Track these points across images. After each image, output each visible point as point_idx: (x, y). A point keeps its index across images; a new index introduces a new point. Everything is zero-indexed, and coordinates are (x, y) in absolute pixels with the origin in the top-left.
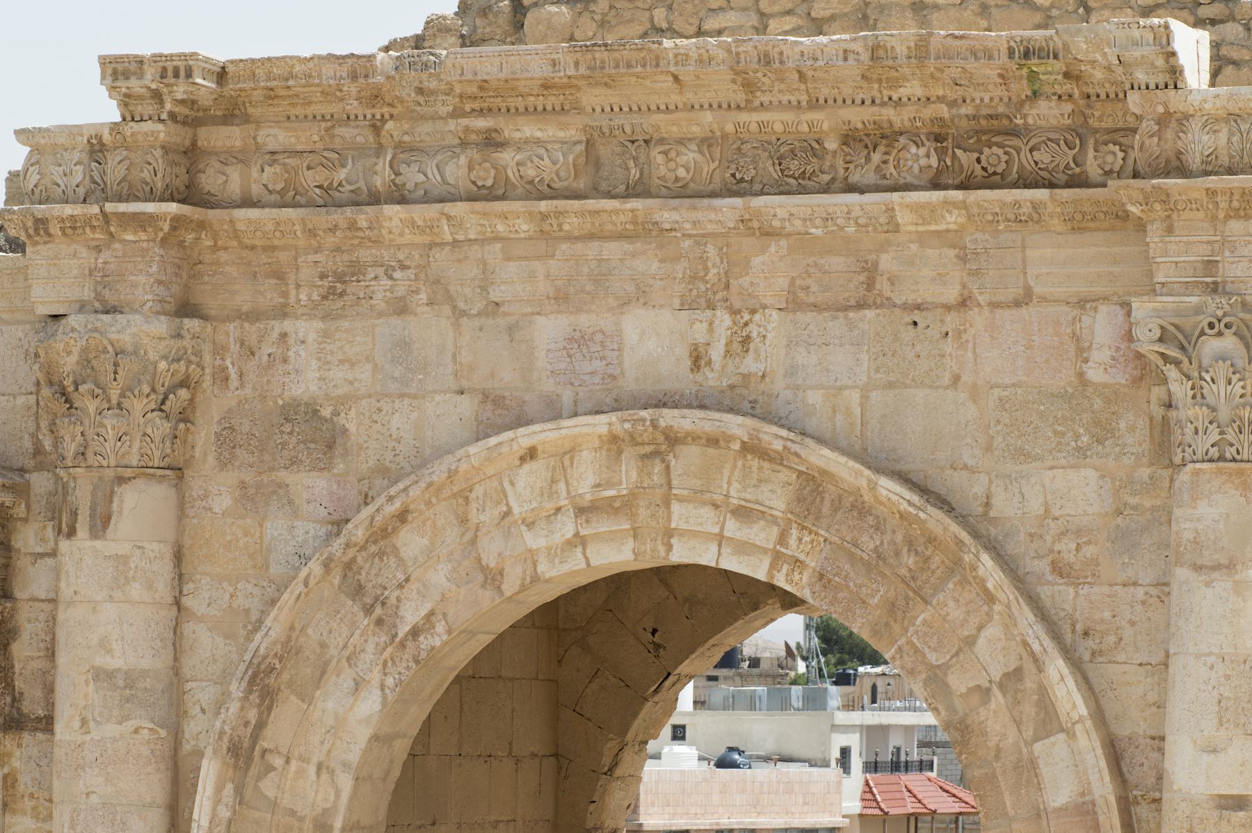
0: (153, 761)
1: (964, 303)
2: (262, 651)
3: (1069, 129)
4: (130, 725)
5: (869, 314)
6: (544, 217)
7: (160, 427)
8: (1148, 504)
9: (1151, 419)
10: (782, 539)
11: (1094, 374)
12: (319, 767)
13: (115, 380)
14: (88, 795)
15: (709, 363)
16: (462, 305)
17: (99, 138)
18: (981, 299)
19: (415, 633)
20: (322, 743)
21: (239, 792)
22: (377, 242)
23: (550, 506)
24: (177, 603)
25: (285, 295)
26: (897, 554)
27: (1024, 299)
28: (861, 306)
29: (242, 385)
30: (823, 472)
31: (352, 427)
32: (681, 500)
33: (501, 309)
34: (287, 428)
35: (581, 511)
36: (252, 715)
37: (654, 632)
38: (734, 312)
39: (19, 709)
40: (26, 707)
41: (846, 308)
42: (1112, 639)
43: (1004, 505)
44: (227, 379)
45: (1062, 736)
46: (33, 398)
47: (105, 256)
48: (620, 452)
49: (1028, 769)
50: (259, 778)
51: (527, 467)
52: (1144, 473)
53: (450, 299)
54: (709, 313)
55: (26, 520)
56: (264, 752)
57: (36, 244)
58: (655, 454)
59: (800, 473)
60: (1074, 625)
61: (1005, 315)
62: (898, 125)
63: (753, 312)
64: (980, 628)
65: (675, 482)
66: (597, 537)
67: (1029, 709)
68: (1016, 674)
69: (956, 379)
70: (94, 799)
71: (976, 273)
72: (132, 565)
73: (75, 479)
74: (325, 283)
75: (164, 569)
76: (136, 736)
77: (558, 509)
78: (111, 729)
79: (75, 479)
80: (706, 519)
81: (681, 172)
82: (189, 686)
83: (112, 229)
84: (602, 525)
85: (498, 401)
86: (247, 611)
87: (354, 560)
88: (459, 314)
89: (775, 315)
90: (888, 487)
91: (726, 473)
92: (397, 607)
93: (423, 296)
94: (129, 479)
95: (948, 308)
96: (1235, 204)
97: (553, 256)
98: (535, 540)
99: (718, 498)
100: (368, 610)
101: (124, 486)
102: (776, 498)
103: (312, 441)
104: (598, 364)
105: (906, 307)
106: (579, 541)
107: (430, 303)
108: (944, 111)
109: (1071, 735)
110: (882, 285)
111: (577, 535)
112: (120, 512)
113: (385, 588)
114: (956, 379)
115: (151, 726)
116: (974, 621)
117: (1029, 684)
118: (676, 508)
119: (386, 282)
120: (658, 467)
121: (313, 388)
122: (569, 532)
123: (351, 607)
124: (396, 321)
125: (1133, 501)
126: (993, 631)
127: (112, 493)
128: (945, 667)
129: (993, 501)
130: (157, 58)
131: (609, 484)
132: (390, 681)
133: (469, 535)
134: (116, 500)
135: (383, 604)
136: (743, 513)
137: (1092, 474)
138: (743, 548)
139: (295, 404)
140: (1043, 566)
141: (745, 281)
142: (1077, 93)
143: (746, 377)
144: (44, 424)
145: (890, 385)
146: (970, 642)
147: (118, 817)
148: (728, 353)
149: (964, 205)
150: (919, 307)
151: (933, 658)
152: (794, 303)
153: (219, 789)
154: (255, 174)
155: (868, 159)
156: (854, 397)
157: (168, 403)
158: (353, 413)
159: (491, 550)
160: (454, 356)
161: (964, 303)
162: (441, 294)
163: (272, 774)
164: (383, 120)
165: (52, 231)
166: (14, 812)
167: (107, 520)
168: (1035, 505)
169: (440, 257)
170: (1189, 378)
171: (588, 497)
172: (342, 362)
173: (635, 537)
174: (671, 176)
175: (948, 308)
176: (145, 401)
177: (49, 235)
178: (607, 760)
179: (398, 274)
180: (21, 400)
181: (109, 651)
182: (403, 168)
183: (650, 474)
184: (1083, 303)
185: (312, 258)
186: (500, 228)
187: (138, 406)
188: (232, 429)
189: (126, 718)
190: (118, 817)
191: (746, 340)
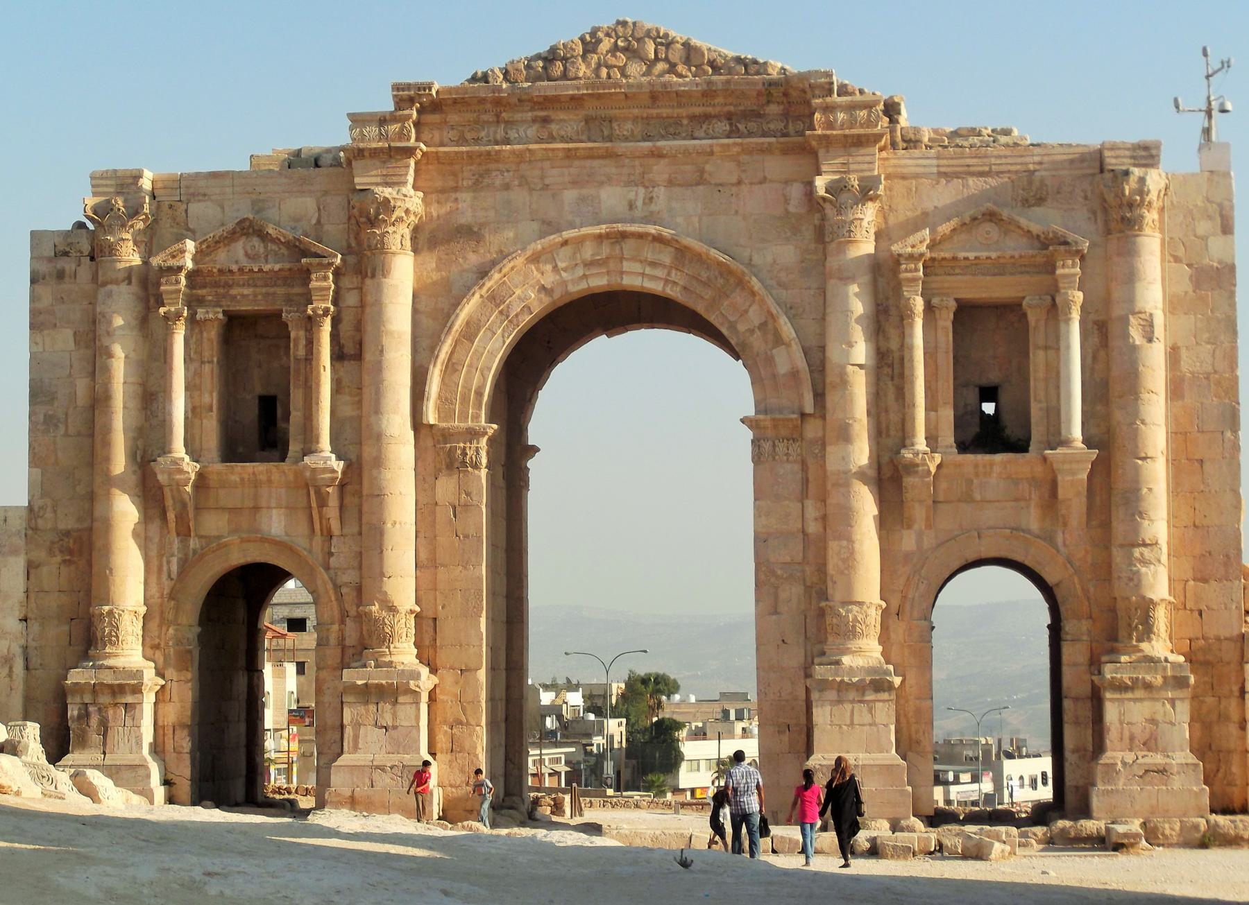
1: (739, 183)
3: (781, 115)
5: (701, 187)
6: (569, 150)
8: (815, 258)
9: (815, 226)
10: (669, 274)
11: (792, 209)
15: (636, 207)
16: (532, 186)
18: (746, 181)
25: (457, 182)
26: (716, 278)
27: (764, 180)
28: (698, 184)
30: (686, 247)
32: (627, 259)
38: (646, 187)
40: (346, 350)
41: (691, 185)
42: (801, 310)
43: (757, 259)
45: (783, 346)
46: (347, 225)
48: (602, 242)
49: (770, 360)
51: (563, 248)
52: (813, 246)
53: (527, 183)
54: (635, 188)
55: (344, 275)
56: (454, 364)
57: (357, 160)
58: (617, 242)
59: (676, 248)
60: (786, 306)
61: (756, 188)
62: (713, 113)
63: (654, 187)
64: (750, 306)
66: (592, 275)
67: (770, 337)
68: (763, 326)
69: (737, 212)
71: (744, 171)
73: (374, 254)
74: (475, 178)
77: (576, 265)
79: (374, 254)
80: (637, 267)
81: (625, 133)
83: (392, 154)
84: (594, 271)
85: (549, 224)
86: (443, 309)
88: (531, 190)
89: (663, 189)
90: (714, 253)
91: (646, 249)
93: (516, 183)
95: (733, 185)
96: (855, 141)
97: (571, 167)
99: (642, 258)
102: (666, 257)
104: (590, 208)
105: (717, 185)
106: (585, 276)
107: (520, 185)
108: (732, 108)
109: (788, 345)
110: (706, 176)
111: (584, 275)
114: (737, 212)
116: (748, 304)
117: (770, 326)
118: (625, 263)
119: (500, 177)
120: (618, 247)
121: (470, 219)
122: (581, 274)
124: (505, 193)
125: (808, 257)
126: (755, 307)
128: (736, 322)
129: (753, 258)
130: (416, 84)
131: (598, 254)
136: (653, 264)
137: (792, 248)
139: (462, 226)
140: (774, 283)
142: (785, 101)
143: (652, 213)
144: (352, 236)
145: (710, 215)
146: (746, 311)
148: (644, 203)
149: (741, 144)
150: (721, 185)
151: (732, 319)
152: (671, 183)
154: (445, 133)
155: (701, 127)
156: (696, 220)
158: (487, 230)
160: (530, 207)
161: (739, 183)
162: (524, 182)
164: (501, 112)
166: (340, 393)
168: (769, 259)
169: (523, 166)
170: (835, 207)
171: (589, 259)
172: (482, 209)
173: (608, 274)
174: (621, 134)
175: (733, 185)
177: (363, 156)
179: (506, 174)
180: (341, 226)
182: (509, 132)
184: (787, 182)
185: (469, 168)
186: (550, 155)
188: (434, 236)
191: (651, 198)
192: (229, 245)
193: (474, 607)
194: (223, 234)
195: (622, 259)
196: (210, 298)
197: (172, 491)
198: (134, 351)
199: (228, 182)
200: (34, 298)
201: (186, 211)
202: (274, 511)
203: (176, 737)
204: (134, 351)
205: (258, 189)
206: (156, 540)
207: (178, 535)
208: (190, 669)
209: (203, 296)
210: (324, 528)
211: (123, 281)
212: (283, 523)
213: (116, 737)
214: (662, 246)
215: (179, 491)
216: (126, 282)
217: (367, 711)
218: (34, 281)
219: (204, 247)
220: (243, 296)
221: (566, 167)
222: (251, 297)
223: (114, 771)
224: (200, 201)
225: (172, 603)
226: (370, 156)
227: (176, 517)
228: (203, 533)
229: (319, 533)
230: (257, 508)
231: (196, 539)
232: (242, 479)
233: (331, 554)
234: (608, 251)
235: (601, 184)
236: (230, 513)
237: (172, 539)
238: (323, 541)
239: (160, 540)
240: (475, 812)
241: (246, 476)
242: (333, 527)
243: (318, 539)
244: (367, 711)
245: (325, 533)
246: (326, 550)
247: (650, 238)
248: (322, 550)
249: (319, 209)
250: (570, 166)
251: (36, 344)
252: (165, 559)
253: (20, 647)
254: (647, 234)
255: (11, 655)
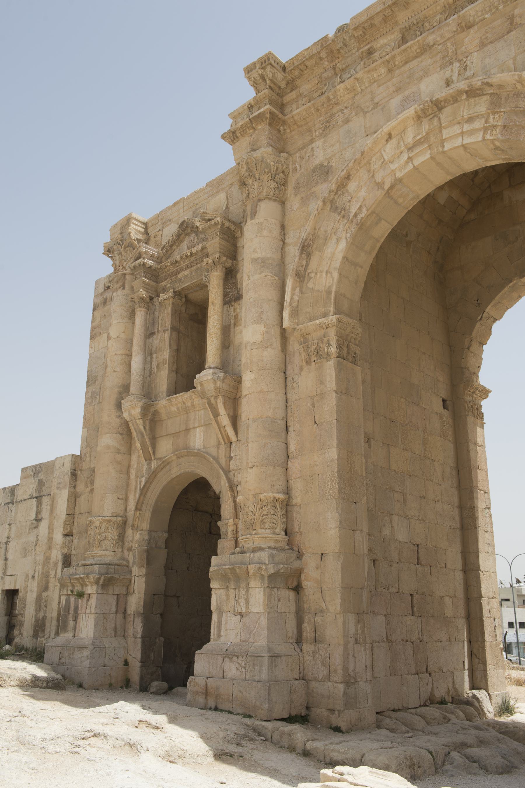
0: (272, 286)
2: (305, 237)
4: (263, 274)
7: (273, 184)
12: (327, 272)
13: (256, 170)
14: (249, 299)
16: (366, 110)
17: (250, 104)
19: (356, 215)
20: (327, 264)
21: (301, 290)
22: (337, 104)
23: (398, 151)
24: (284, 243)
25: (312, 136)
29: (301, 169)
31: (334, 164)
33: (379, 104)
34: (314, 174)
35: (410, 149)
36: (304, 263)
37: (477, 301)
38: (459, 61)
39: (239, 293)
44: (296, 170)
47: (254, 136)
48: (421, 122)
50: (307, 283)
51: (389, 144)
59: (491, 94)
63: (467, 57)
65: (442, 122)
70: (252, 300)
72: (264, 225)
75: (276, 230)
76: (265, 278)
78: (257, 276)
80: (457, 129)
82: (287, 266)
84: (417, 150)
87: (334, 198)
91: (461, 109)
92: (349, 209)
94: (263, 200)
98: (393, 167)
100: (339, 214)
101: (261, 202)
103: (322, 174)
106: (410, 159)
110: (517, 20)
112: (260, 210)
113: (345, 204)
115: (272, 275)
118: (444, 132)
119: (341, 115)
120: (436, 120)
121: (322, 159)
123: (335, 216)
127: (257, 205)
131: (419, 134)
132: (348, 235)
133: (371, 175)
134: (258, 207)
135: (344, 209)
138: (471, 133)
141: (463, 49)
147: (259, 304)
153: (293, 289)
157: (276, 178)
159: (378, 178)
163: (312, 280)
165: (238, 136)
167: (255, 213)
172: (330, 147)
173: (430, 149)
176: (267, 176)
177: (237, 137)
178: (466, 344)
180: (240, 204)
181: (256, 252)
183: (433, 124)
187: (265, 178)
188: (298, 183)
189: (263, 272)
190: (259, 304)
192: (179, 246)
193: (330, 489)
194: (173, 238)
195: (441, 128)
196: (169, 285)
197: (133, 424)
198: (124, 332)
199: (181, 205)
200: (93, 320)
201: (162, 236)
202: (198, 430)
203: (135, 623)
204: (124, 332)
205: (196, 203)
206: (135, 466)
207: (146, 461)
208: (145, 566)
209: (165, 286)
210: (225, 438)
211: (120, 288)
212: (202, 439)
213: (81, 622)
214: (477, 99)
215: (137, 424)
216: (122, 288)
217: (228, 595)
218: (94, 310)
219: (164, 251)
220: (186, 276)
221: (389, 81)
222: (189, 276)
223: (71, 652)
224: (168, 225)
225: (138, 513)
226: (241, 135)
227: (141, 446)
228: (158, 455)
229: (223, 443)
230: (188, 430)
231: (155, 461)
232: (178, 409)
233: (231, 458)
234: (427, 127)
235: (421, 79)
236: (173, 437)
237: (143, 463)
238: (226, 448)
239: (137, 466)
240: (336, 712)
241: (180, 405)
242: (229, 434)
243: (223, 447)
244: (228, 595)
245: (227, 442)
246: (228, 455)
247: (464, 97)
248: (225, 456)
249: (227, 198)
250: (393, 77)
251: (92, 348)
252: (139, 479)
253: (62, 554)
254: (460, 92)
255: (57, 561)
